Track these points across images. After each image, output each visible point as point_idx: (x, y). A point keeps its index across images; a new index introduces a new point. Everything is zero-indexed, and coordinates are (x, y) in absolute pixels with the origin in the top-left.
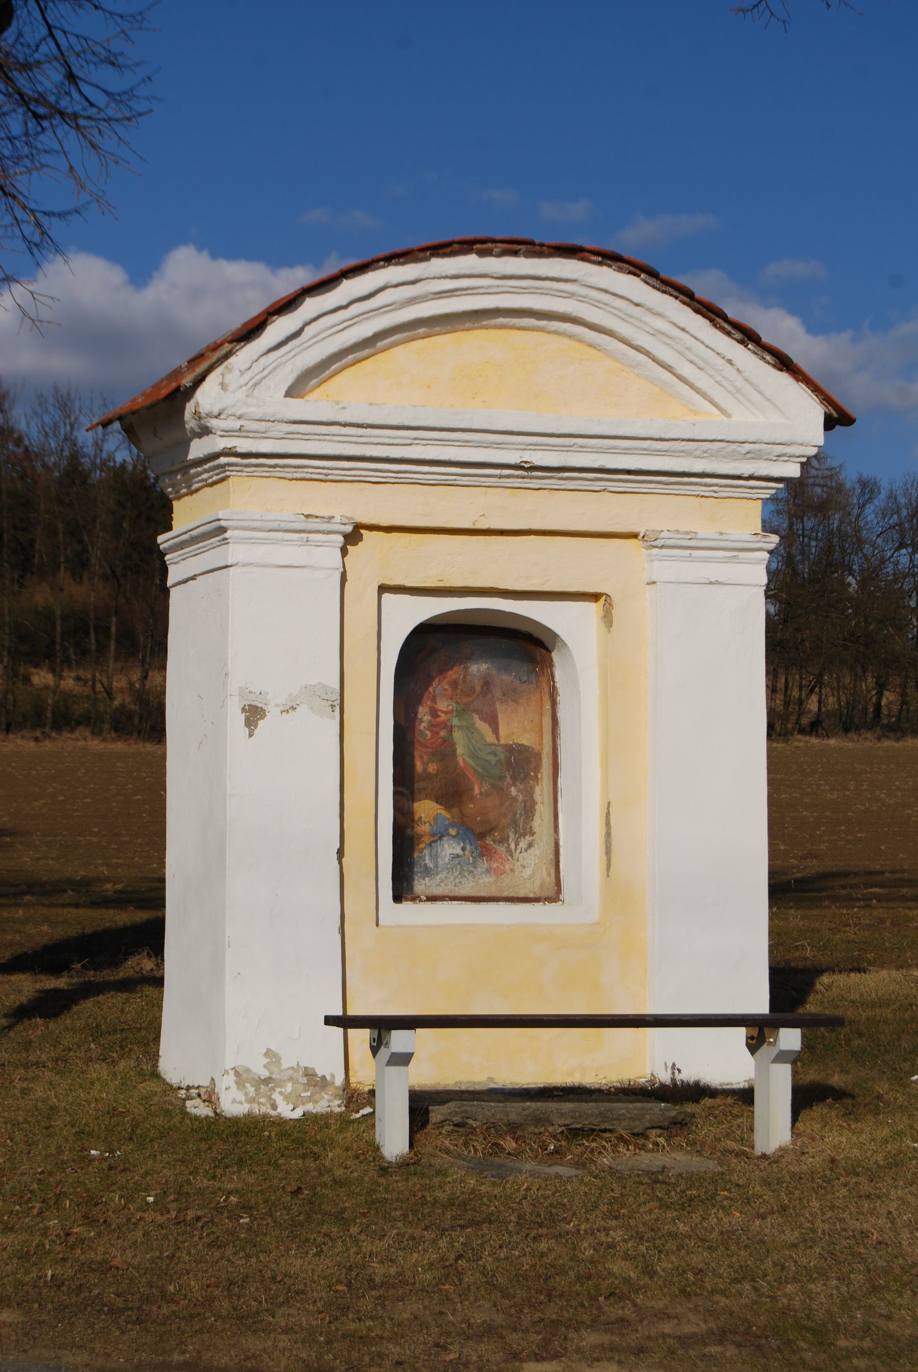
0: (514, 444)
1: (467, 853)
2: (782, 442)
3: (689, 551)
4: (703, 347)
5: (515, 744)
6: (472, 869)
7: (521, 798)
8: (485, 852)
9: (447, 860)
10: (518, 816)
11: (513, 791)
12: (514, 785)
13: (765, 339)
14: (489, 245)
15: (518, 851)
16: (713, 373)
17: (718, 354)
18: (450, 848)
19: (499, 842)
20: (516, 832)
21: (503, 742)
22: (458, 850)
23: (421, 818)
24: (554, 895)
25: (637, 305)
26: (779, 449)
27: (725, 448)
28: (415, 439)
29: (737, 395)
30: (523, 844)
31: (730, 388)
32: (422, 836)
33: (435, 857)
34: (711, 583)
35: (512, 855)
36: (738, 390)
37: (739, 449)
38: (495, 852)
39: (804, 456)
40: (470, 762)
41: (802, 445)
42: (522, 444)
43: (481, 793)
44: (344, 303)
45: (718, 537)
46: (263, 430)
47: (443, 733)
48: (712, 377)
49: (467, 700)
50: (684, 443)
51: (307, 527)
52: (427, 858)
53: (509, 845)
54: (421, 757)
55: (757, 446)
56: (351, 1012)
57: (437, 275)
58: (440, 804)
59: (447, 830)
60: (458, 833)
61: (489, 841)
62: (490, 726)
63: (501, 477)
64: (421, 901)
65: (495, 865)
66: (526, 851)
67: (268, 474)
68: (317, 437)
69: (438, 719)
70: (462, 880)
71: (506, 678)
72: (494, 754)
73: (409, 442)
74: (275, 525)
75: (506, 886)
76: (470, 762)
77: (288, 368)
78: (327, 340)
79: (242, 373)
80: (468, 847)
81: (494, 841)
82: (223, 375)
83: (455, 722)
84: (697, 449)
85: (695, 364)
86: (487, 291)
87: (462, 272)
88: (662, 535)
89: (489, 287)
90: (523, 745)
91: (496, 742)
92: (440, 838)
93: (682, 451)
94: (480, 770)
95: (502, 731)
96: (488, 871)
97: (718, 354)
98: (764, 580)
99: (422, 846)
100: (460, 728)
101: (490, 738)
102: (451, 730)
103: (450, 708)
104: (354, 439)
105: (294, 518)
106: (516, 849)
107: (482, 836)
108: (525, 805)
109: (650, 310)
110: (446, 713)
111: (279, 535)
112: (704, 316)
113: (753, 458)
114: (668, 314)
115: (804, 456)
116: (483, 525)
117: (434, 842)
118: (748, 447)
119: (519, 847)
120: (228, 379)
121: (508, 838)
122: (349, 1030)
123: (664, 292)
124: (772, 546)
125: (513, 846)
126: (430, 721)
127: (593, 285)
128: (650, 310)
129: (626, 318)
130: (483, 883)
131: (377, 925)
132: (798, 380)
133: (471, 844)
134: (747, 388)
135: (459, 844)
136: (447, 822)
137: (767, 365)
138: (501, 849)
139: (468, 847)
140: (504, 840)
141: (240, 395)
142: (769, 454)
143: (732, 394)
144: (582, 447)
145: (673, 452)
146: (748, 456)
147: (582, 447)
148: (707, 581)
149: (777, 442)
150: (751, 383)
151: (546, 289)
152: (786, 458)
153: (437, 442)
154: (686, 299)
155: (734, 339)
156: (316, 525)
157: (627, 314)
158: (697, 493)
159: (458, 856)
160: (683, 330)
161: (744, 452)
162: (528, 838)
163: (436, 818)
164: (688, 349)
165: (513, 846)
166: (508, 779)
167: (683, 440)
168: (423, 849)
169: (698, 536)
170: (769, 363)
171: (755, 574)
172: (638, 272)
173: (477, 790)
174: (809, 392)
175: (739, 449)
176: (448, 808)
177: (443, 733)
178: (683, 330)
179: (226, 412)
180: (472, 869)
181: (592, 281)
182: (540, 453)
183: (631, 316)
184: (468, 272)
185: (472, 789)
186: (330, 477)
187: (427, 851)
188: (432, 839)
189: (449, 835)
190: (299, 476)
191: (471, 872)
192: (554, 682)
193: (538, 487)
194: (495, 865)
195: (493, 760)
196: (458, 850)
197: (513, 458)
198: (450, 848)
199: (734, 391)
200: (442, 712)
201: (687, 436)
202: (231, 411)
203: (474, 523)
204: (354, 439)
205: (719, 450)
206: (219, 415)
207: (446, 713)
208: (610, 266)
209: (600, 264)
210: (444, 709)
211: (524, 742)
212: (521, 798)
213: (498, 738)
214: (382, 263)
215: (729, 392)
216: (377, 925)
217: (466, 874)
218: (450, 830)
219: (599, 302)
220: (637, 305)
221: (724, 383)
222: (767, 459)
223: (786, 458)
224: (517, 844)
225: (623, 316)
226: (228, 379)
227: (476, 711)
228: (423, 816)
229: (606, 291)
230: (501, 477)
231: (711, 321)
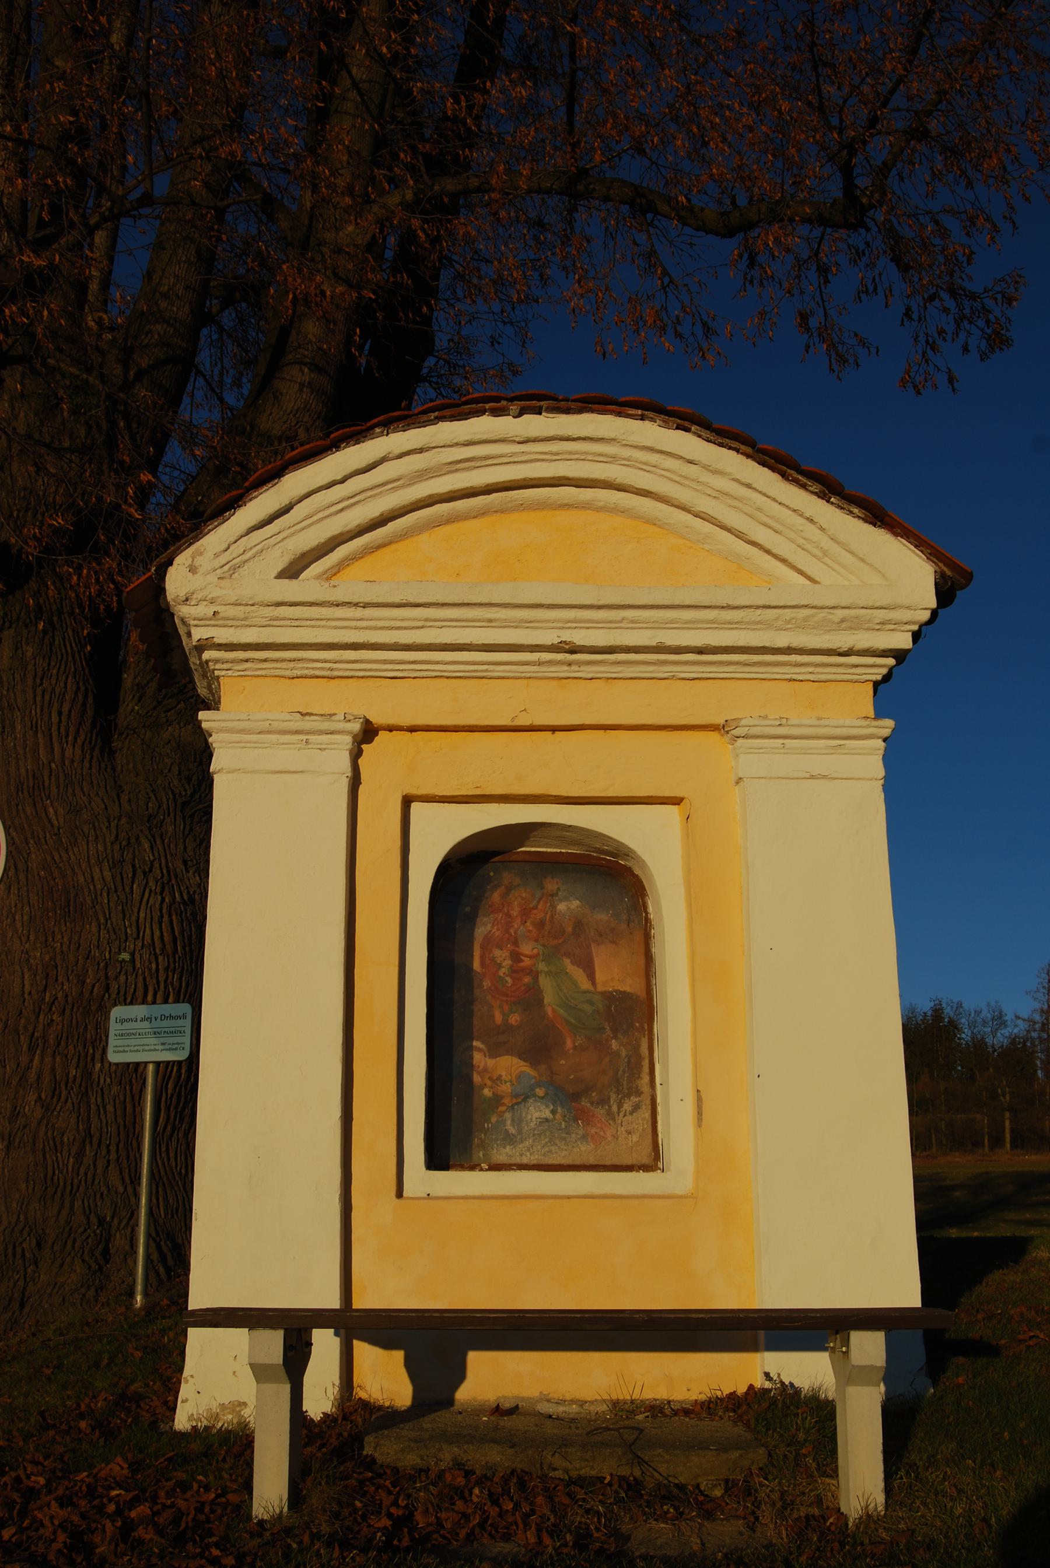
0: (548, 621)
1: (558, 1116)
2: (883, 604)
3: (781, 741)
4: (776, 505)
5: (616, 991)
6: (564, 1135)
7: (624, 1053)
8: (580, 1116)
9: (532, 1125)
10: (620, 1072)
11: (614, 1044)
12: (615, 1037)
13: (849, 490)
14: (504, 403)
15: (622, 1114)
16: (792, 535)
17: (794, 511)
18: (537, 1112)
19: (598, 1104)
20: (618, 1092)
21: (600, 988)
22: (547, 1114)
23: (500, 1076)
24: (653, 1162)
25: (690, 462)
26: (881, 614)
27: (813, 616)
28: (426, 620)
29: (826, 560)
30: (627, 1106)
31: (816, 551)
32: (502, 1097)
33: (518, 1122)
34: (812, 777)
35: (614, 1119)
36: (825, 553)
37: (831, 617)
38: (593, 1116)
39: (914, 623)
40: (561, 1011)
41: (908, 608)
42: (559, 621)
43: (575, 1048)
44: (339, 477)
45: (815, 722)
46: (242, 616)
47: (527, 980)
48: (792, 541)
49: (555, 942)
50: (759, 612)
51: (306, 725)
52: (509, 1122)
53: (610, 1106)
54: (501, 1007)
55: (853, 613)
56: (362, 1301)
57: (448, 443)
58: (525, 1060)
59: (533, 1090)
60: (547, 1094)
61: (585, 1103)
62: (584, 970)
63: (540, 663)
64: (481, 1170)
65: (593, 1131)
66: (631, 1113)
67: (263, 672)
68: (309, 623)
69: (522, 964)
70: (553, 1148)
71: (602, 917)
72: (591, 1002)
73: (420, 624)
74: (265, 725)
75: (607, 1154)
76: (561, 1011)
77: (277, 552)
78: (325, 522)
79: (216, 556)
80: (559, 1110)
81: (592, 1103)
82: (193, 558)
83: (542, 966)
84: (777, 619)
85: (770, 527)
86: (511, 459)
87: (477, 437)
88: (743, 722)
89: (513, 455)
90: (624, 992)
91: (592, 988)
92: (525, 1100)
93: (759, 623)
94: (573, 1021)
95: (599, 976)
96: (584, 1137)
97: (794, 511)
98: (881, 772)
99: (501, 1109)
100: (548, 974)
101: (585, 984)
102: (536, 978)
103: (535, 951)
104: (353, 624)
105: (288, 717)
106: (619, 1113)
107: (575, 1097)
108: (629, 1062)
109: (706, 467)
110: (531, 957)
111: (274, 737)
112: (773, 469)
113: (851, 628)
114: (728, 470)
115: (914, 623)
116: (524, 721)
117: (517, 1104)
118: (840, 614)
119: (623, 1109)
120: (199, 561)
121: (609, 1099)
122: (197, 1301)
123: (721, 445)
124: (887, 732)
125: (615, 1108)
126: (511, 967)
127: (635, 444)
128: (706, 467)
129: (683, 481)
130: (584, 1151)
131: (400, 1194)
132: (896, 535)
133: (563, 1107)
134: (835, 549)
135: (547, 1106)
136: (533, 1081)
137: (856, 520)
138: (600, 1112)
139: (559, 1110)
140: (604, 1101)
141: (213, 578)
142: (869, 621)
143: (819, 559)
144: (632, 622)
145: (748, 623)
146: (843, 625)
147: (632, 622)
148: (807, 775)
149: (877, 604)
150: (838, 543)
151: (581, 453)
152: (893, 627)
153: (454, 624)
154: (749, 450)
155: (812, 493)
156: (315, 723)
157: (681, 476)
158: (788, 677)
159: (547, 1120)
160: (749, 486)
161: (837, 620)
162: (634, 1099)
163: (519, 1077)
164: (759, 509)
165: (615, 1108)
166: (608, 1032)
167: (758, 607)
168: (504, 1112)
169: (789, 723)
170: (859, 517)
171: (871, 764)
172: (687, 424)
173: (569, 1044)
174: (912, 547)
175: (831, 617)
176: (534, 1064)
177: (527, 980)
178: (749, 486)
179: (195, 596)
180: (564, 1135)
181: (635, 439)
182: (583, 632)
183: (687, 478)
184: (485, 437)
185: (564, 1042)
186: (336, 673)
187: (508, 1115)
188: (514, 1101)
189: (535, 1095)
190: (299, 673)
191: (563, 1139)
192: (647, 913)
193: (590, 676)
194: (593, 1131)
195: (588, 1008)
196: (547, 1114)
197: (549, 637)
198: (537, 1112)
199: (820, 554)
200: (526, 956)
201: (761, 603)
202: (200, 595)
203: (513, 719)
204: (353, 624)
205: (806, 619)
206: (187, 600)
207: (531, 957)
208: (653, 420)
209: (642, 418)
210: (527, 953)
211: (628, 989)
212: (624, 1053)
213: (594, 984)
214: (378, 430)
215: (815, 556)
216: (400, 1194)
217: (557, 1142)
218: (537, 1090)
219: (645, 464)
220: (690, 462)
221: (808, 546)
222: (868, 629)
223: (893, 627)
224: (620, 1106)
225: (678, 479)
226: (199, 561)
227: (568, 955)
228: (504, 1074)
229: (651, 449)
230: (540, 663)
231: (783, 475)
